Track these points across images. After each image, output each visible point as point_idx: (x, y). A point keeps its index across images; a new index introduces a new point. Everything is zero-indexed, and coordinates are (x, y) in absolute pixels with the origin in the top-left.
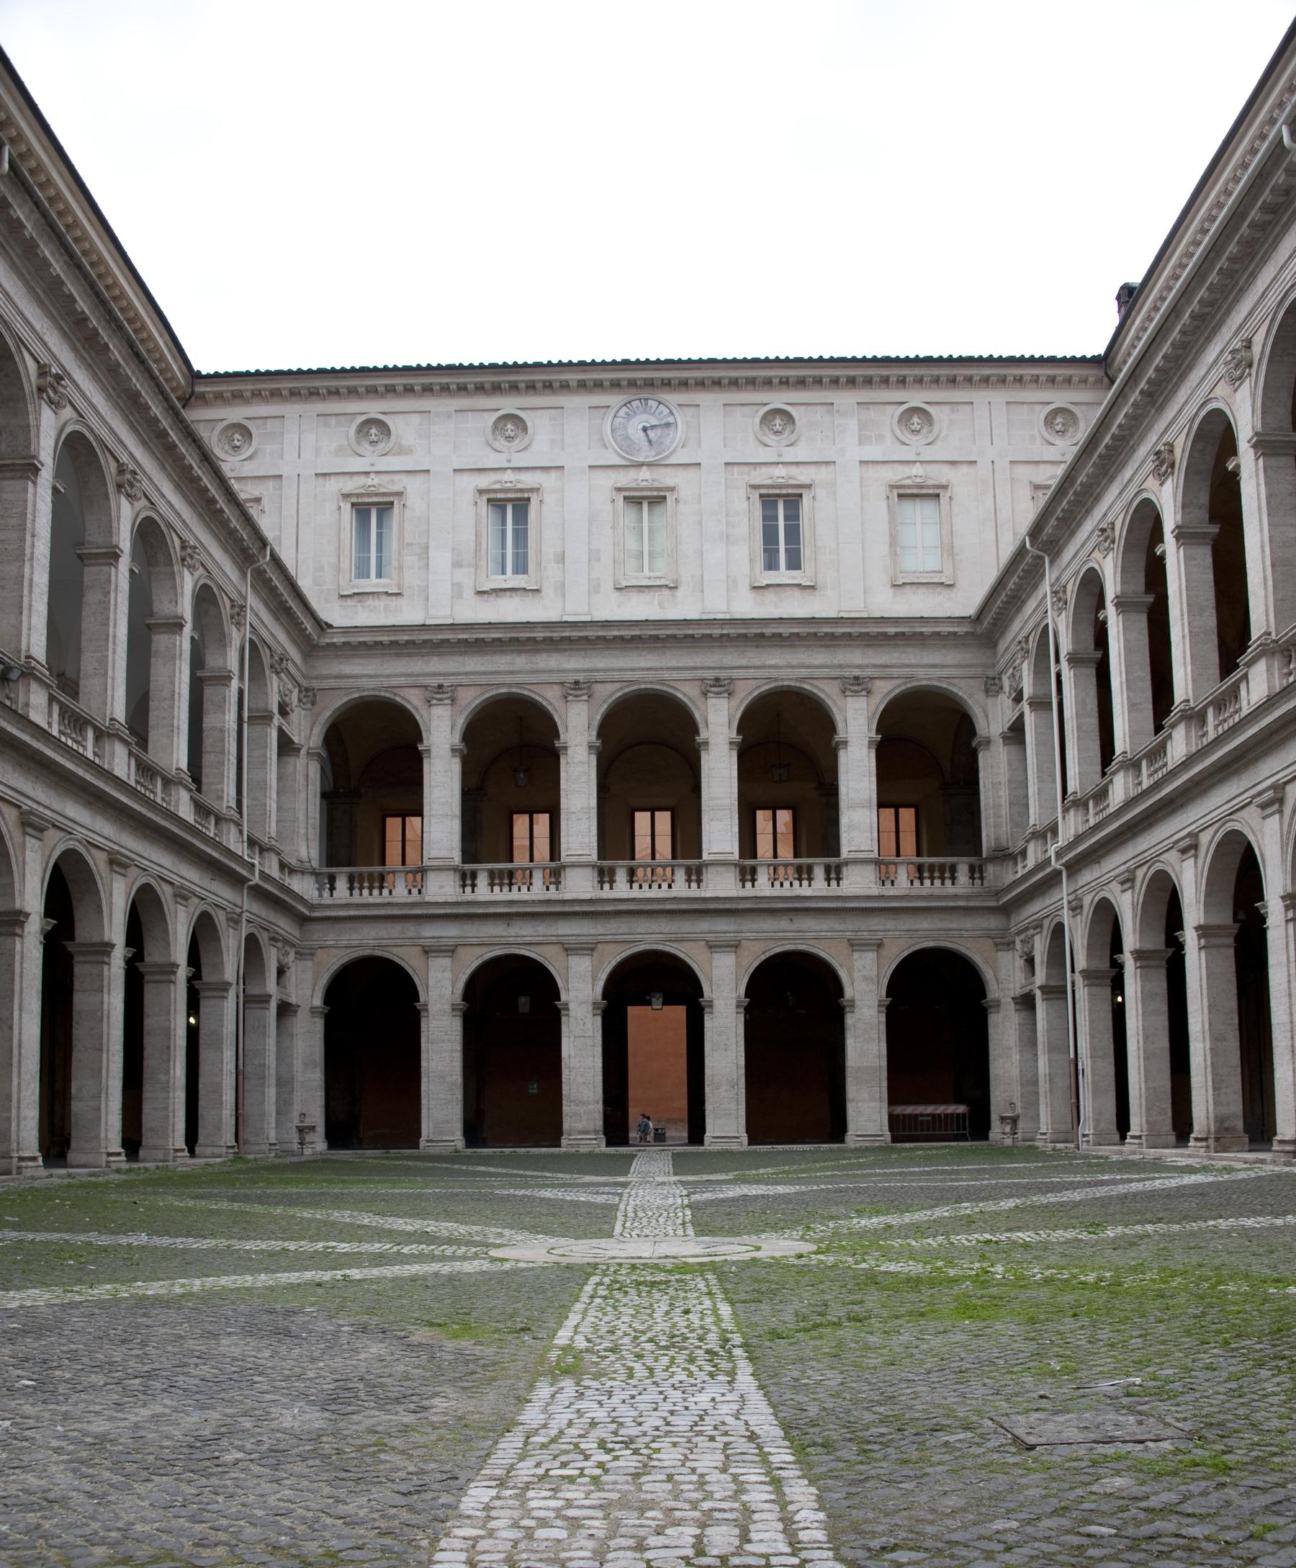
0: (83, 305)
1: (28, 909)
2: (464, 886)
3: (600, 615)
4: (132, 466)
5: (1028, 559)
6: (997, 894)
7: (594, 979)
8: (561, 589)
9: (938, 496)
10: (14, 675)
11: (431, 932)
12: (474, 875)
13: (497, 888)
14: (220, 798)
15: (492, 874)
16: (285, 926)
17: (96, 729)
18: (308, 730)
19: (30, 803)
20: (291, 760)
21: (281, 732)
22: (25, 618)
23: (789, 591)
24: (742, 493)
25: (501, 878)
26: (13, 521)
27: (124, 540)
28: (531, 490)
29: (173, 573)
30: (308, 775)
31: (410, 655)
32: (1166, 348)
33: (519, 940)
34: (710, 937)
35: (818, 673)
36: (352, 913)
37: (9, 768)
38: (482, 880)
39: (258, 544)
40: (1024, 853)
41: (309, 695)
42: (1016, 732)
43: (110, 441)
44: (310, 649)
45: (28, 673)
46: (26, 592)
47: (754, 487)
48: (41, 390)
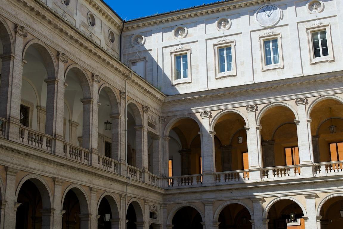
11: (205, 196)
13: (227, 180)
23: (324, 64)
33: (236, 198)
34: (305, 193)
36: (179, 191)
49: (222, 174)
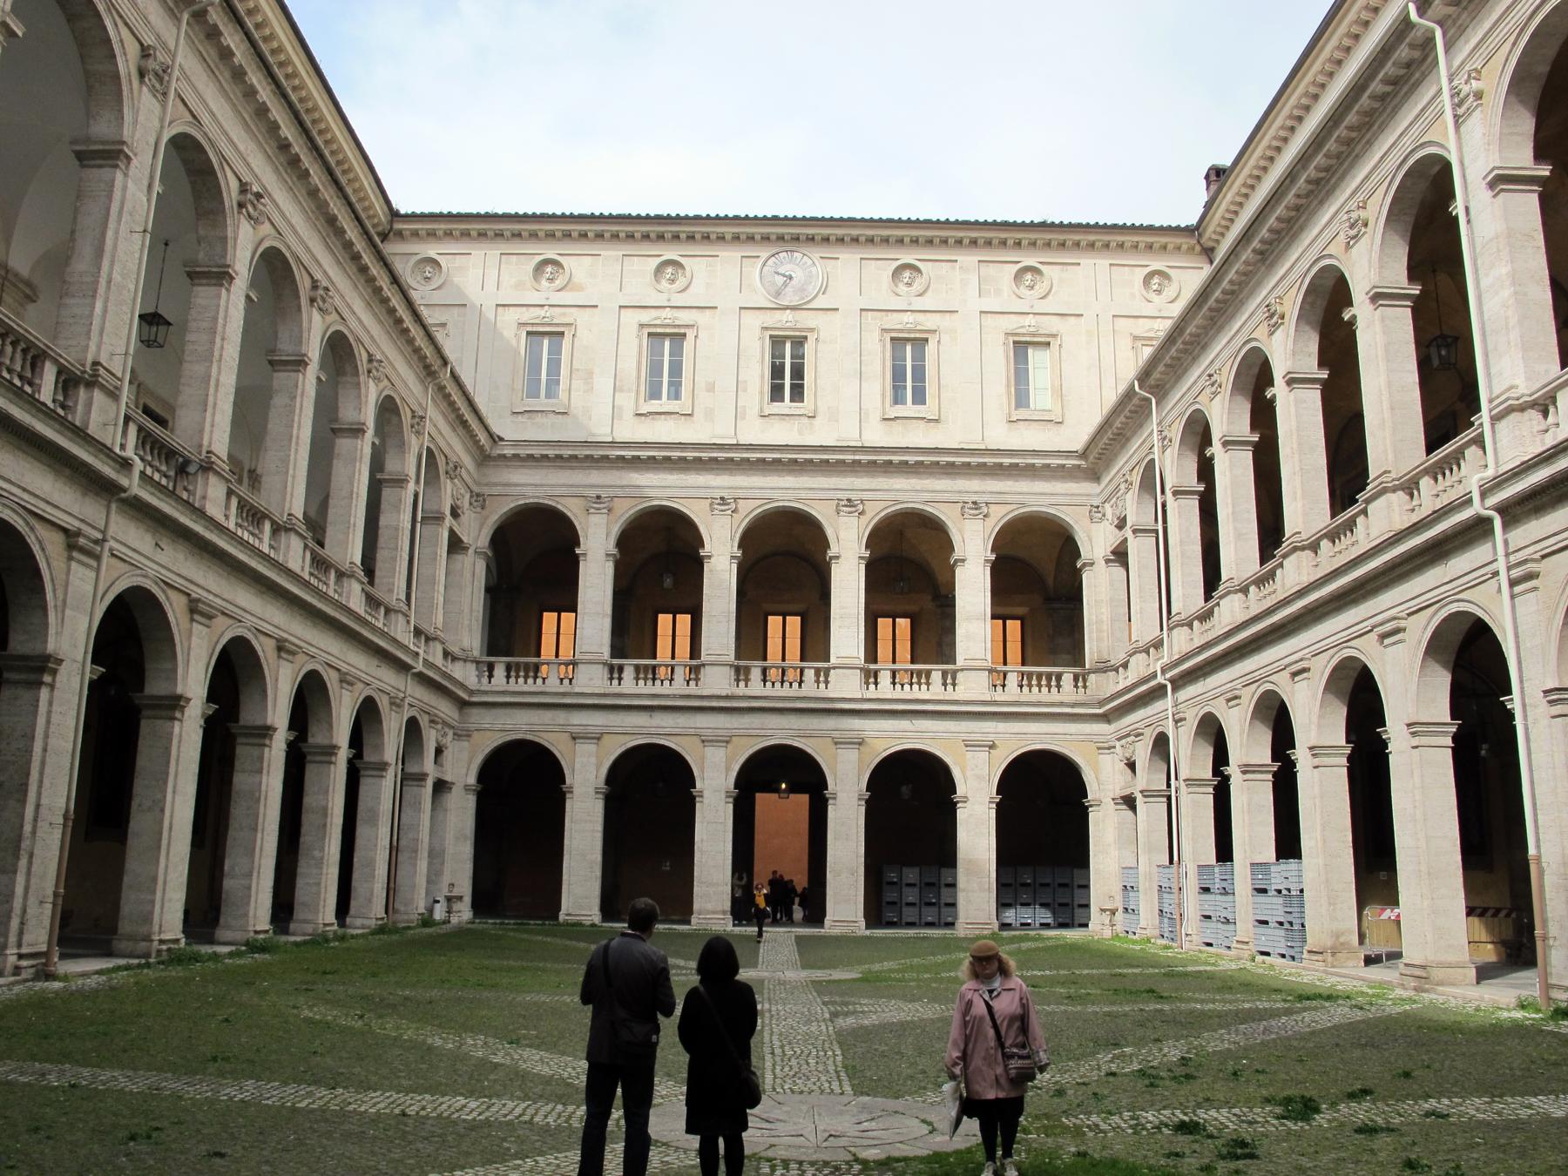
0: (288, 131)
1: (189, 695)
2: (611, 679)
3: (745, 439)
4: (325, 283)
5: (1135, 401)
6: (1101, 703)
7: (728, 769)
8: (710, 414)
9: (1048, 344)
10: (192, 469)
11: (579, 719)
12: (621, 669)
13: (641, 682)
14: (391, 591)
15: (637, 668)
16: (445, 709)
17: (273, 523)
18: (477, 532)
19: (200, 591)
20: (459, 557)
21: (452, 533)
22: (208, 414)
24: (877, 335)
25: (646, 673)
26: (205, 325)
27: (314, 350)
28: (687, 326)
29: (359, 384)
30: (474, 572)
31: (572, 468)
32: (1280, 211)
34: (836, 734)
35: (939, 497)
37: (181, 556)
38: (629, 673)
39: (439, 362)
40: (1125, 666)
41: (479, 500)
42: (1120, 555)
43: (305, 258)
44: (485, 459)
45: (207, 467)
46: (212, 390)
47: (884, 330)
48: (241, 205)
49: (629, 665)
